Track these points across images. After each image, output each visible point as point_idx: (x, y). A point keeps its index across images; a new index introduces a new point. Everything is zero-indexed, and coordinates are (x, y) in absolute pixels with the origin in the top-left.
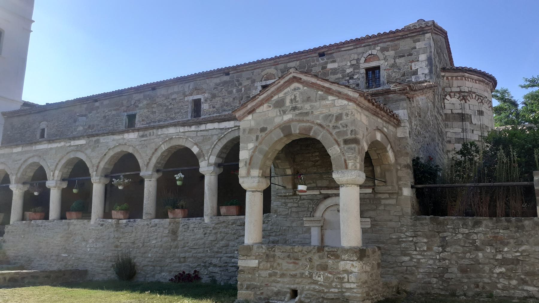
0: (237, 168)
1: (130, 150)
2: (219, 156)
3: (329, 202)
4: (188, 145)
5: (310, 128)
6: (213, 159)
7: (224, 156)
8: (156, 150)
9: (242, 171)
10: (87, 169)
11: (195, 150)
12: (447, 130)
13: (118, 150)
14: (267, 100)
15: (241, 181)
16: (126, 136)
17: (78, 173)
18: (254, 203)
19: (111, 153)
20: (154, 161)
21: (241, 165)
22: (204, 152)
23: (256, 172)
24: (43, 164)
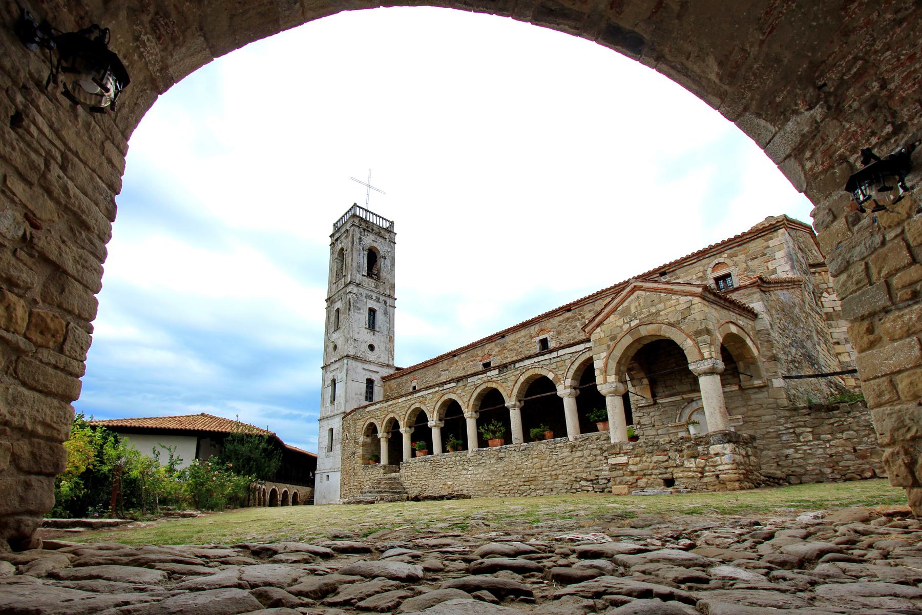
0: (593, 378)
1: (494, 385)
3: (694, 405)
5: (660, 329)
9: (599, 379)
10: (460, 407)
12: (831, 330)
13: (484, 387)
14: (614, 311)
15: (599, 388)
16: (489, 374)
17: (452, 411)
18: (614, 407)
19: (479, 390)
20: (515, 391)
21: (597, 373)
23: (612, 378)
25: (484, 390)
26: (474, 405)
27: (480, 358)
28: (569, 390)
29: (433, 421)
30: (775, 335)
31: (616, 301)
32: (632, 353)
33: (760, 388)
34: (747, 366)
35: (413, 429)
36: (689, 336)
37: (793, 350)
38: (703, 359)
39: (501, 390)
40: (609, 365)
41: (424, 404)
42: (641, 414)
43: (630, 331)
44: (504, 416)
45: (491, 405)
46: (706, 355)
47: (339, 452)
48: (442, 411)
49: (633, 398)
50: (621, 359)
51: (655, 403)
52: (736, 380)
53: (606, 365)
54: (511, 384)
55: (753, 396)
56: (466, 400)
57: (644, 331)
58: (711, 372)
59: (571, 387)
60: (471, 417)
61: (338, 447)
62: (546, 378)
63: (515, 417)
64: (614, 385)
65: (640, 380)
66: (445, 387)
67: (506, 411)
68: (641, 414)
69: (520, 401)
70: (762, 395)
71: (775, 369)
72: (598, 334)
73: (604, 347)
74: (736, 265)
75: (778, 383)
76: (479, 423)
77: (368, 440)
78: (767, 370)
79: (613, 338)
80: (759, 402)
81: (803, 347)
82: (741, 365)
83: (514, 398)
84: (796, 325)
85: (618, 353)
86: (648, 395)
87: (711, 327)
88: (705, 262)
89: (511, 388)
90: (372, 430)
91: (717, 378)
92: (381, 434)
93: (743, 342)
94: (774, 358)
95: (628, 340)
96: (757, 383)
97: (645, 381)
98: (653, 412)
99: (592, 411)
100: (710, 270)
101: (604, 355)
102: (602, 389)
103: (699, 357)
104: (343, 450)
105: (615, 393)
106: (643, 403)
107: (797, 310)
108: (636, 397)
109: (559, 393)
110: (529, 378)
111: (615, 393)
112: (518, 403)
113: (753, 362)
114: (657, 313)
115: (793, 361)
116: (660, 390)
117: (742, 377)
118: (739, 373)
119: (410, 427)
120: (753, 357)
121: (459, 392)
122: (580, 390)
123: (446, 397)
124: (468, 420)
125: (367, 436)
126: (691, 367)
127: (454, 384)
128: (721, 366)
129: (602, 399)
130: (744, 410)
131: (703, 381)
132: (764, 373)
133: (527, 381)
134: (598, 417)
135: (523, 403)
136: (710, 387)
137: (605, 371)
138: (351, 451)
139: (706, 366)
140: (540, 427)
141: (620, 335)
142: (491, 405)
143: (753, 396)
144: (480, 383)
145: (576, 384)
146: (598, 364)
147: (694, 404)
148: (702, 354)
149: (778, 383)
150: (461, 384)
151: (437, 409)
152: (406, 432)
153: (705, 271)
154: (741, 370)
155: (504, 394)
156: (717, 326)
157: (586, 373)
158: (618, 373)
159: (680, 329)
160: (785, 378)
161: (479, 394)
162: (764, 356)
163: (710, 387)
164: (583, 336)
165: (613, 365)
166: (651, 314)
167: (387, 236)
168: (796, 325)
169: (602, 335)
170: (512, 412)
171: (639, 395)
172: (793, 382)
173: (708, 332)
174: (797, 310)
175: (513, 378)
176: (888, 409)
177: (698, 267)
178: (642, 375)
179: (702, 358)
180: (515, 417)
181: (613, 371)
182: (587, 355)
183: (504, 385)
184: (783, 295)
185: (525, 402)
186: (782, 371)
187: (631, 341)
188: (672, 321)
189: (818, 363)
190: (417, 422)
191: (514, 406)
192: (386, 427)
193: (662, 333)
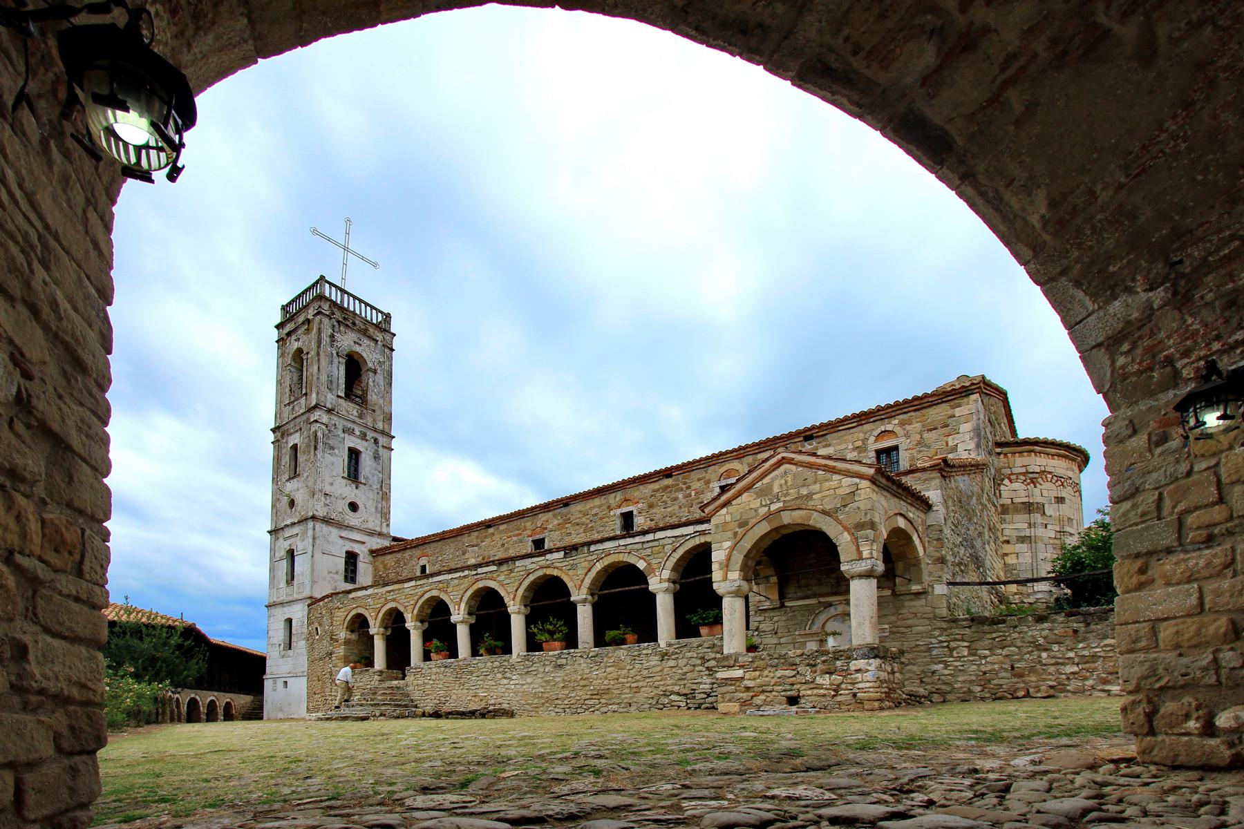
1: (556, 573)
2: (674, 570)
4: (631, 560)
6: (666, 574)
7: (681, 569)
8: (589, 570)
9: (717, 575)
10: (502, 599)
11: (641, 565)
13: (540, 573)
15: (715, 586)
19: (532, 578)
20: (587, 582)
21: (715, 567)
22: (655, 566)
23: (735, 575)
24: (444, 597)
25: (539, 578)
26: (524, 597)
27: (529, 532)
28: (666, 585)
29: (459, 615)
30: (947, 531)
31: (754, 475)
32: (765, 544)
33: (918, 594)
34: (907, 568)
35: (426, 625)
36: (846, 529)
37: (962, 551)
38: (861, 558)
39: (566, 579)
40: (733, 558)
41: (446, 592)
42: (761, 618)
43: (768, 517)
44: (569, 613)
45: (549, 601)
46: (865, 554)
47: (304, 651)
48: (473, 603)
49: (753, 599)
50: (750, 551)
51: (782, 606)
52: (890, 584)
53: (729, 558)
54: (581, 572)
55: (907, 604)
56: (511, 589)
57: (787, 518)
58: (868, 575)
59: (669, 580)
60: (519, 613)
61: (300, 645)
62: (632, 568)
63: (584, 616)
64: (737, 584)
65: (767, 577)
66: (480, 571)
67: (573, 607)
68: (761, 618)
69: (592, 595)
70: (918, 604)
71: (940, 573)
72: (723, 516)
73: (729, 534)
74: (907, 436)
75: (940, 589)
76: (529, 620)
77: (354, 637)
78: (930, 574)
79: (741, 525)
80: (913, 610)
81: (973, 547)
82: (900, 566)
83: (584, 590)
84: (970, 519)
85: (747, 544)
86: (775, 596)
87: (876, 520)
88: (867, 427)
89: (581, 577)
90: (359, 624)
91: (874, 582)
92: (375, 629)
93: (910, 538)
94: (942, 561)
95: (764, 528)
96: (915, 588)
97: (774, 579)
98: (779, 619)
99: (695, 612)
100: (872, 439)
101: (728, 544)
102: (719, 586)
103: (855, 556)
104: (311, 648)
105: (737, 593)
106: (767, 605)
107: (974, 500)
108: (758, 598)
109: (651, 588)
110: (609, 566)
111: (737, 593)
112: (590, 597)
113: (916, 562)
114: (809, 496)
115: (960, 564)
116: (791, 590)
117: (898, 580)
118: (895, 576)
119: (422, 622)
120: (917, 559)
121: (501, 578)
122: (681, 584)
123: (480, 585)
124: (513, 616)
125: (352, 631)
126: (842, 568)
127: (494, 568)
128: (880, 567)
129: (717, 601)
130: (894, 618)
131: (855, 585)
132: (926, 578)
133: (605, 569)
134: (703, 619)
135: (596, 598)
136: (863, 594)
137: (726, 566)
138: (325, 650)
139: (863, 567)
140: (618, 629)
141: (754, 521)
142: (549, 601)
143: (907, 604)
144: (536, 568)
145: (675, 576)
146: (717, 556)
147: (832, 609)
148: (859, 552)
149: (940, 589)
150: (504, 568)
151: (465, 599)
152: (415, 628)
153: (865, 440)
154: (898, 572)
155: (570, 585)
156: (884, 518)
157: (696, 565)
158: (744, 568)
159: (837, 520)
160: (949, 584)
161: (532, 583)
162: (930, 557)
163: (863, 594)
164: (698, 514)
165: (738, 559)
166: (800, 497)
167: (379, 336)
168: (970, 519)
169: (728, 518)
170: (580, 608)
171: (764, 595)
172: (955, 589)
173: (872, 525)
174: (974, 500)
175: (586, 564)
176: (1141, 656)
177: (858, 434)
178: (770, 571)
179: (859, 557)
180: (584, 616)
181: (738, 566)
182: (702, 539)
183: (571, 573)
184: (962, 482)
185: (599, 596)
186: (947, 576)
187: (768, 529)
188: (828, 507)
189: (983, 566)
190: (432, 615)
191: (585, 601)
192: (383, 619)
193: (811, 523)
